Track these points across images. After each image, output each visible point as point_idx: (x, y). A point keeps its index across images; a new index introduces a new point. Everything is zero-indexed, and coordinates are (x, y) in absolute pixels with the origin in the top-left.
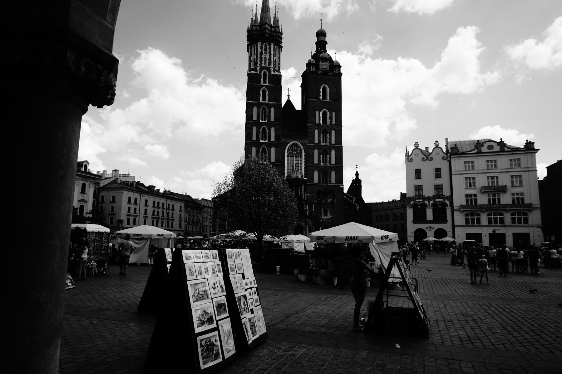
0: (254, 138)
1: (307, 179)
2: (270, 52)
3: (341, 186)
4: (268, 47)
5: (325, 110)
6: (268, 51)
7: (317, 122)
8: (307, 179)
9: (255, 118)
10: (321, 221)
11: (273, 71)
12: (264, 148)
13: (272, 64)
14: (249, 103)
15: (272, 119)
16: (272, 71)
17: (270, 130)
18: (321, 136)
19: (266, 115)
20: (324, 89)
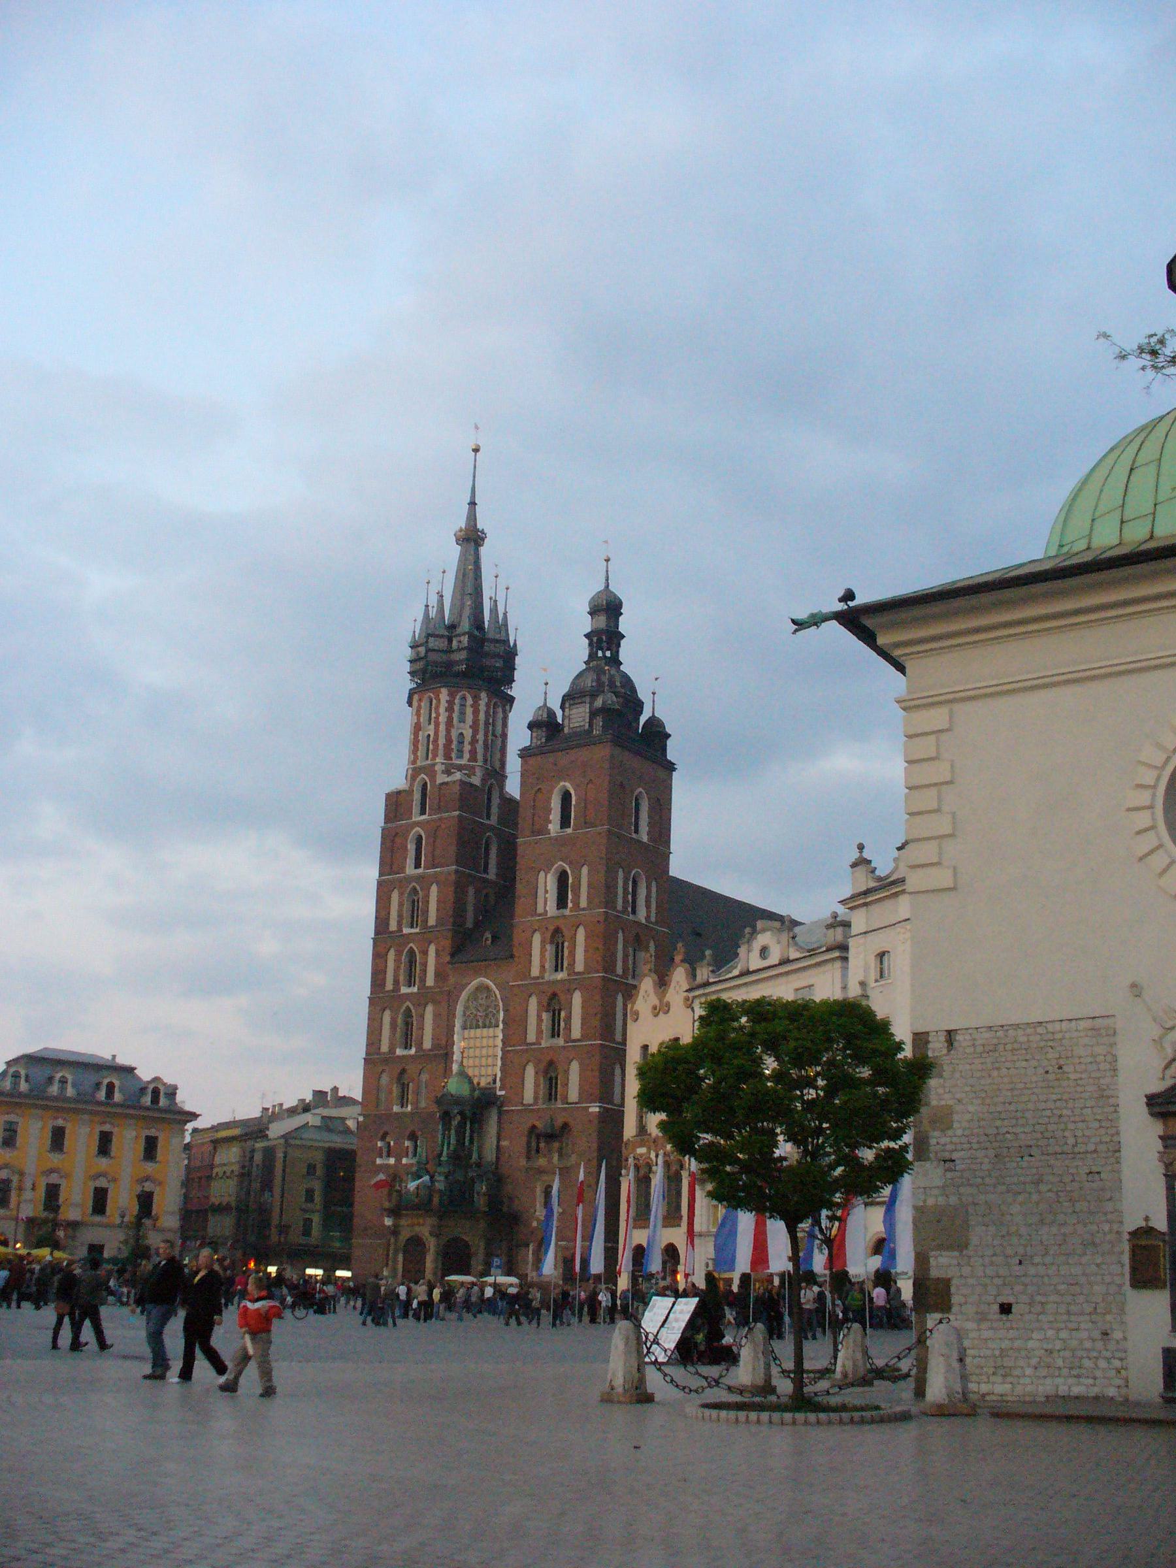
0: (389, 986)
1: (503, 1093)
2: (438, 715)
3: (591, 1110)
4: (434, 701)
5: (560, 865)
6: (434, 715)
7: (540, 909)
8: (503, 1093)
9: (393, 926)
10: (535, 1224)
11: (448, 772)
12: (408, 1010)
13: (441, 752)
14: (384, 881)
15: (432, 921)
16: (439, 772)
17: (425, 953)
18: (546, 950)
19: (416, 912)
20: (566, 797)
